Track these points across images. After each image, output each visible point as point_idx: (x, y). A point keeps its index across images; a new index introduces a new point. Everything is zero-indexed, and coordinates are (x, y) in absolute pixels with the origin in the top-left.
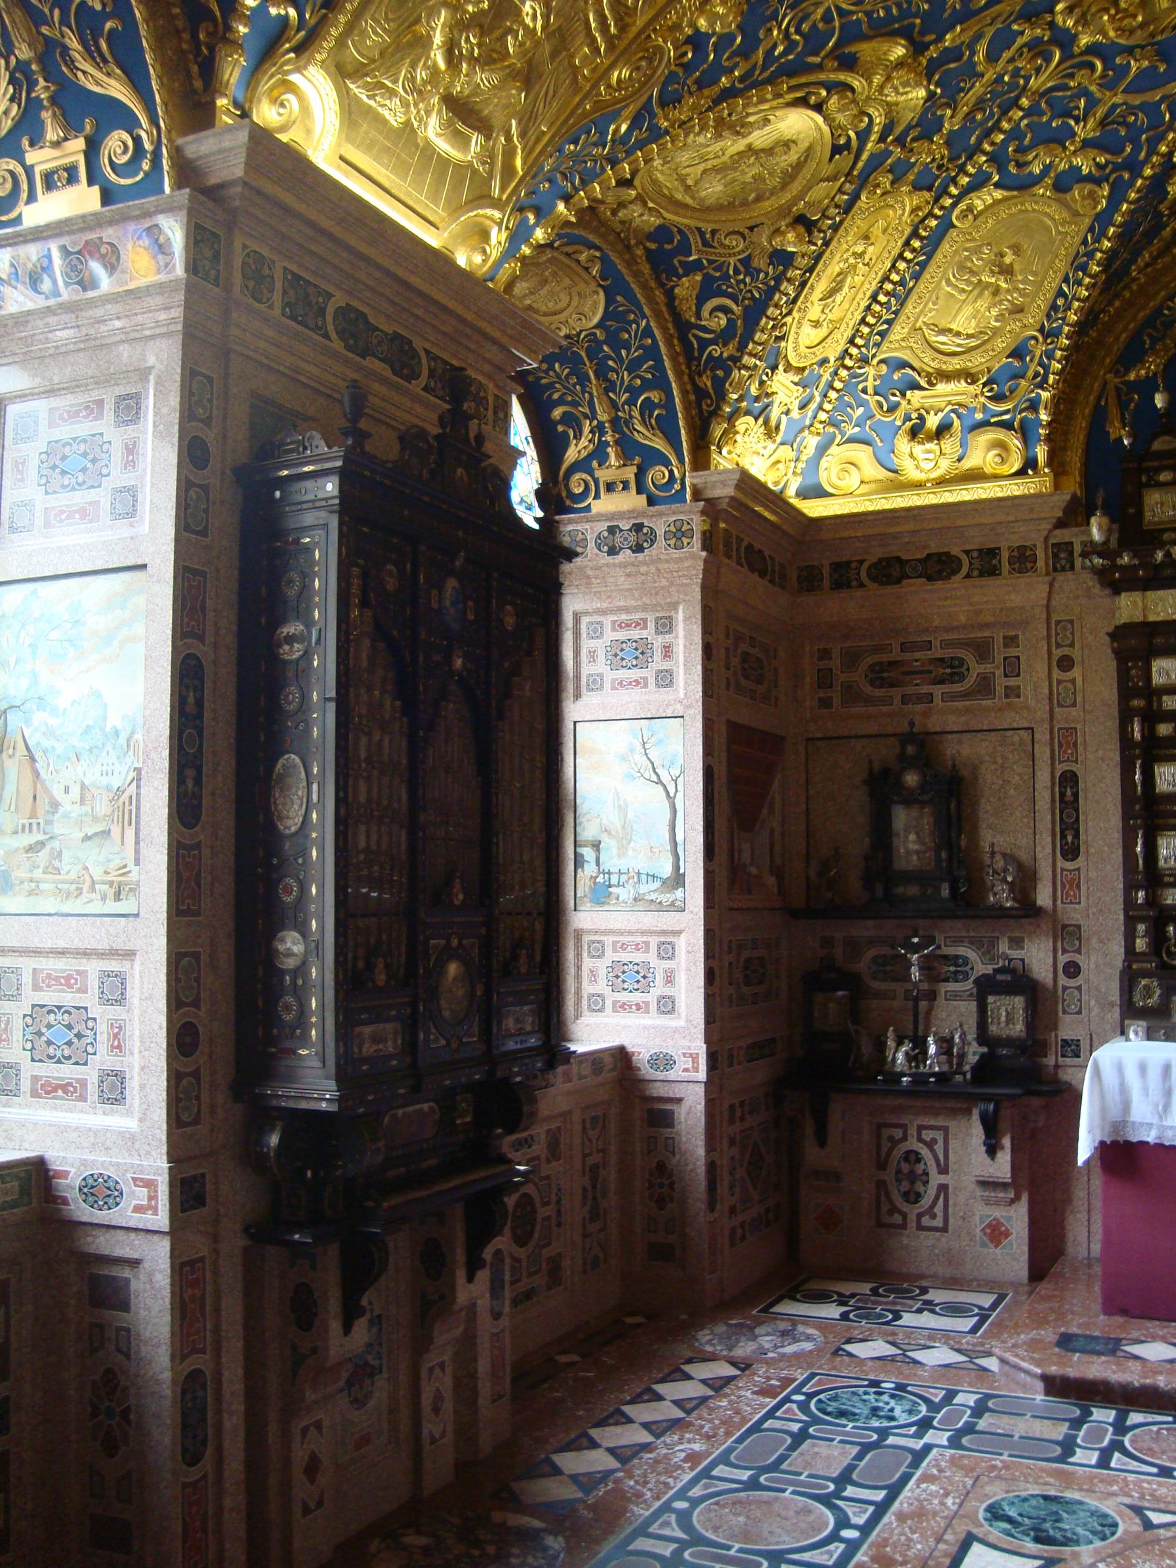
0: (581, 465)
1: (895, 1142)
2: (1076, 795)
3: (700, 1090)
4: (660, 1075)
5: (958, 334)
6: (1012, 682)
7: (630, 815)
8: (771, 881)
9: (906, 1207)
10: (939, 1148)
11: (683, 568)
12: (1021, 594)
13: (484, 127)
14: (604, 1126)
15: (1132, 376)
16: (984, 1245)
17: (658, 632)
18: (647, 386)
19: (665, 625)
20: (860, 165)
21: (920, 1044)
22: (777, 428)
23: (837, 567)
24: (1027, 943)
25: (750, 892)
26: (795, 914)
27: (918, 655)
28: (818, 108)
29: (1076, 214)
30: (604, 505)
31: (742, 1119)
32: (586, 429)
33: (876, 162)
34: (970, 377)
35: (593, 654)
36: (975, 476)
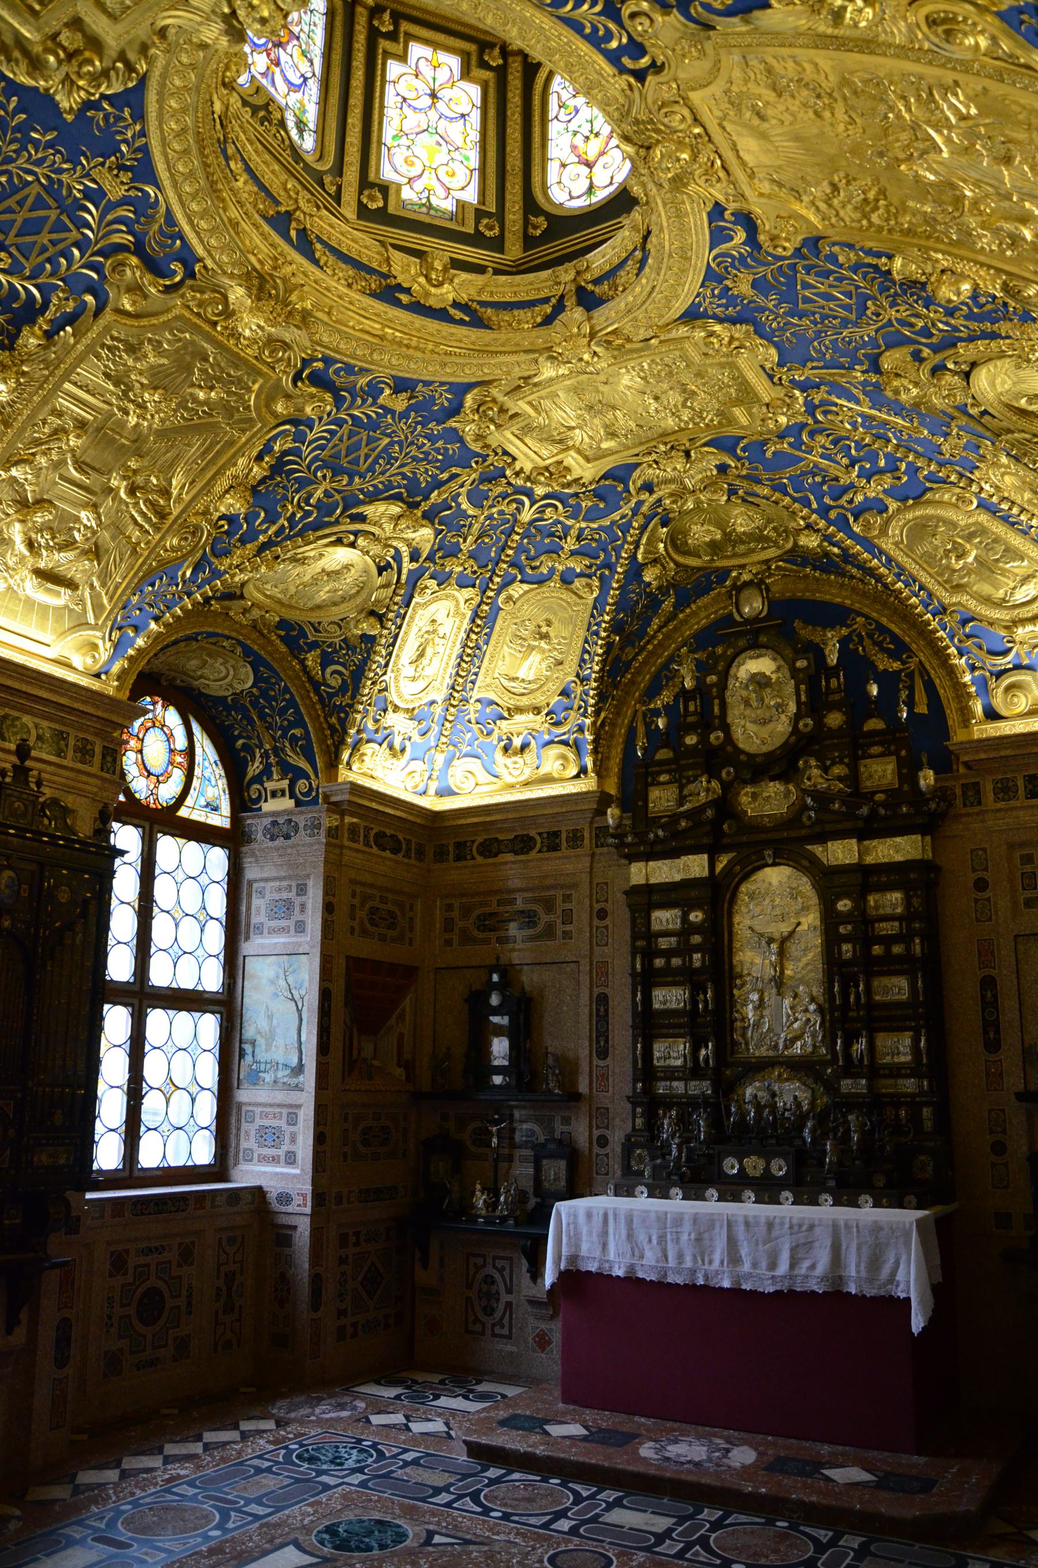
0: (258, 779)
2: (606, 1011)
3: (307, 1220)
4: (283, 1209)
5: (523, 681)
6: (568, 928)
7: (275, 1022)
8: (399, 1072)
11: (310, 849)
12: (570, 864)
13: (71, 584)
14: (242, 1243)
15: (652, 706)
16: (534, 1351)
17: (298, 895)
18: (292, 725)
19: (302, 890)
20: (404, 577)
21: (497, 1196)
22: (403, 750)
23: (459, 845)
24: (573, 1121)
25: (371, 1079)
27: (508, 908)
28: (353, 545)
29: (581, 598)
30: (269, 806)
31: (357, 1244)
32: (258, 755)
33: (415, 577)
34: (537, 710)
35: (258, 909)
36: (548, 779)
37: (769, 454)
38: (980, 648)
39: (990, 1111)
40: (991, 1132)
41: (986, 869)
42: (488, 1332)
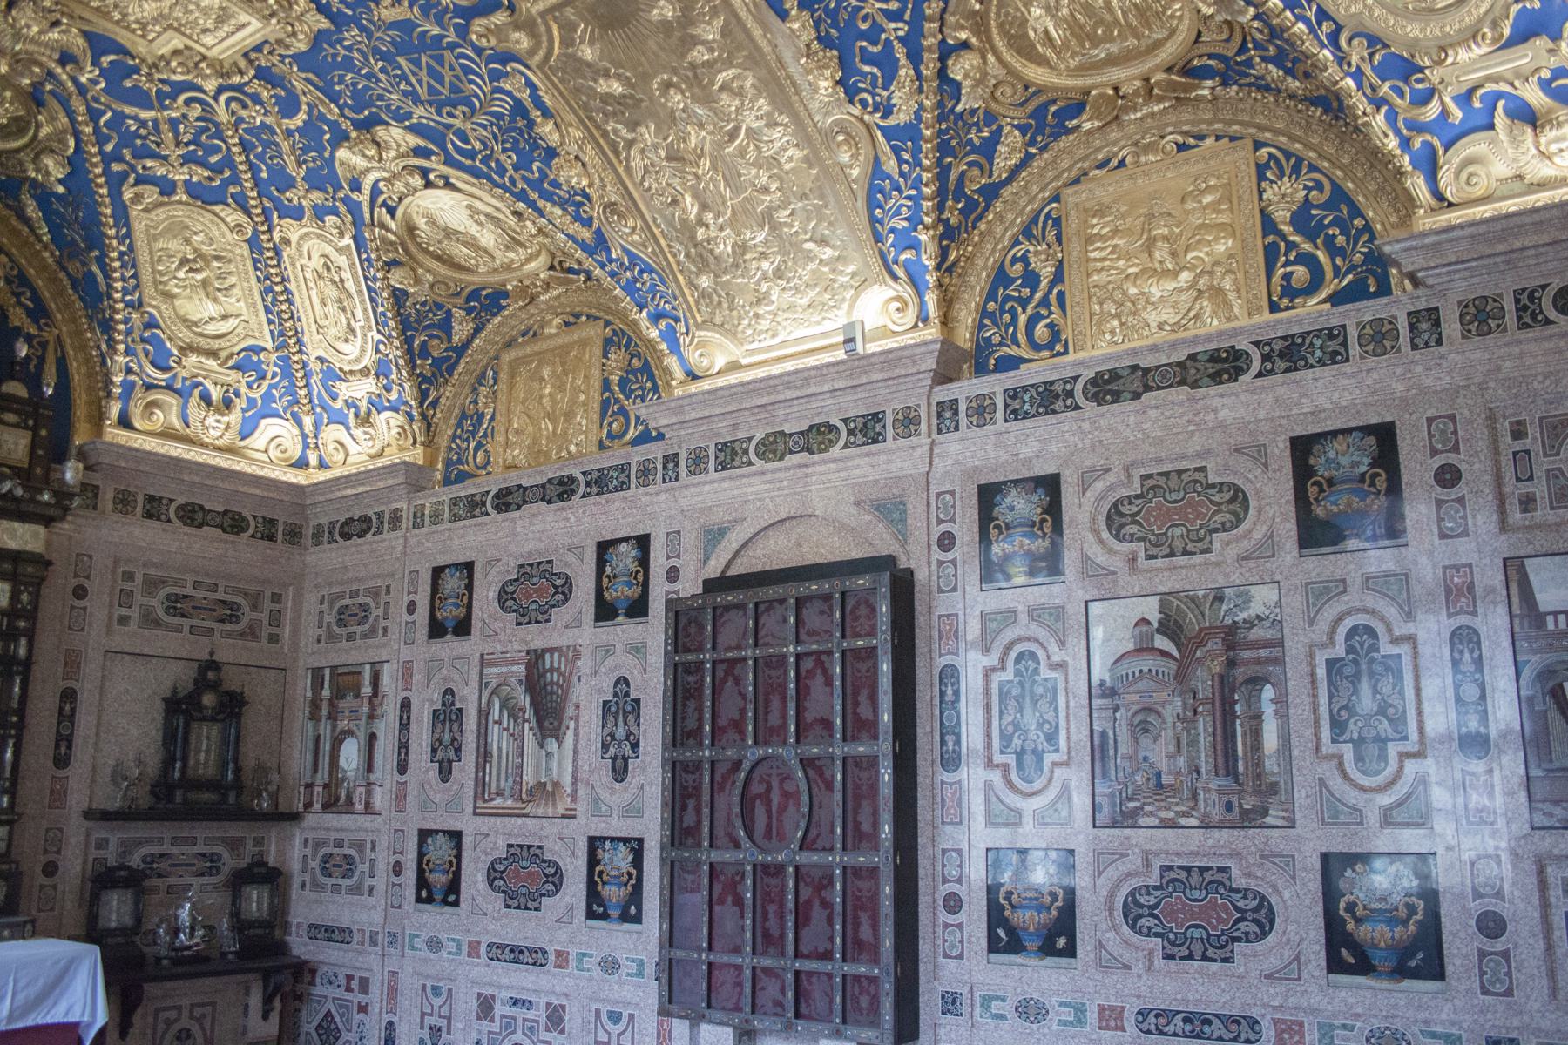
37: (128, 84)
38: (147, 353)
39: (47, 830)
40: (46, 852)
41: (88, 577)
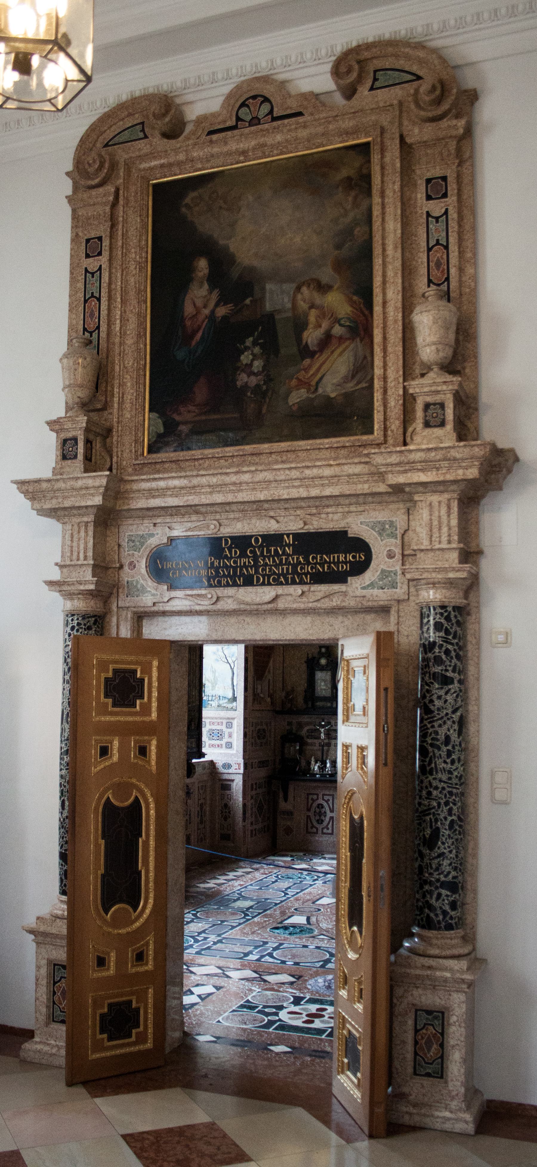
1: (313, 801)
3: (241, 777)
7: (217, 674)
8: (269, 700)
9: (317, 826)
10: (330, 803)
21: (324, 763)
26: (277, 712)
42: (320, 832)
